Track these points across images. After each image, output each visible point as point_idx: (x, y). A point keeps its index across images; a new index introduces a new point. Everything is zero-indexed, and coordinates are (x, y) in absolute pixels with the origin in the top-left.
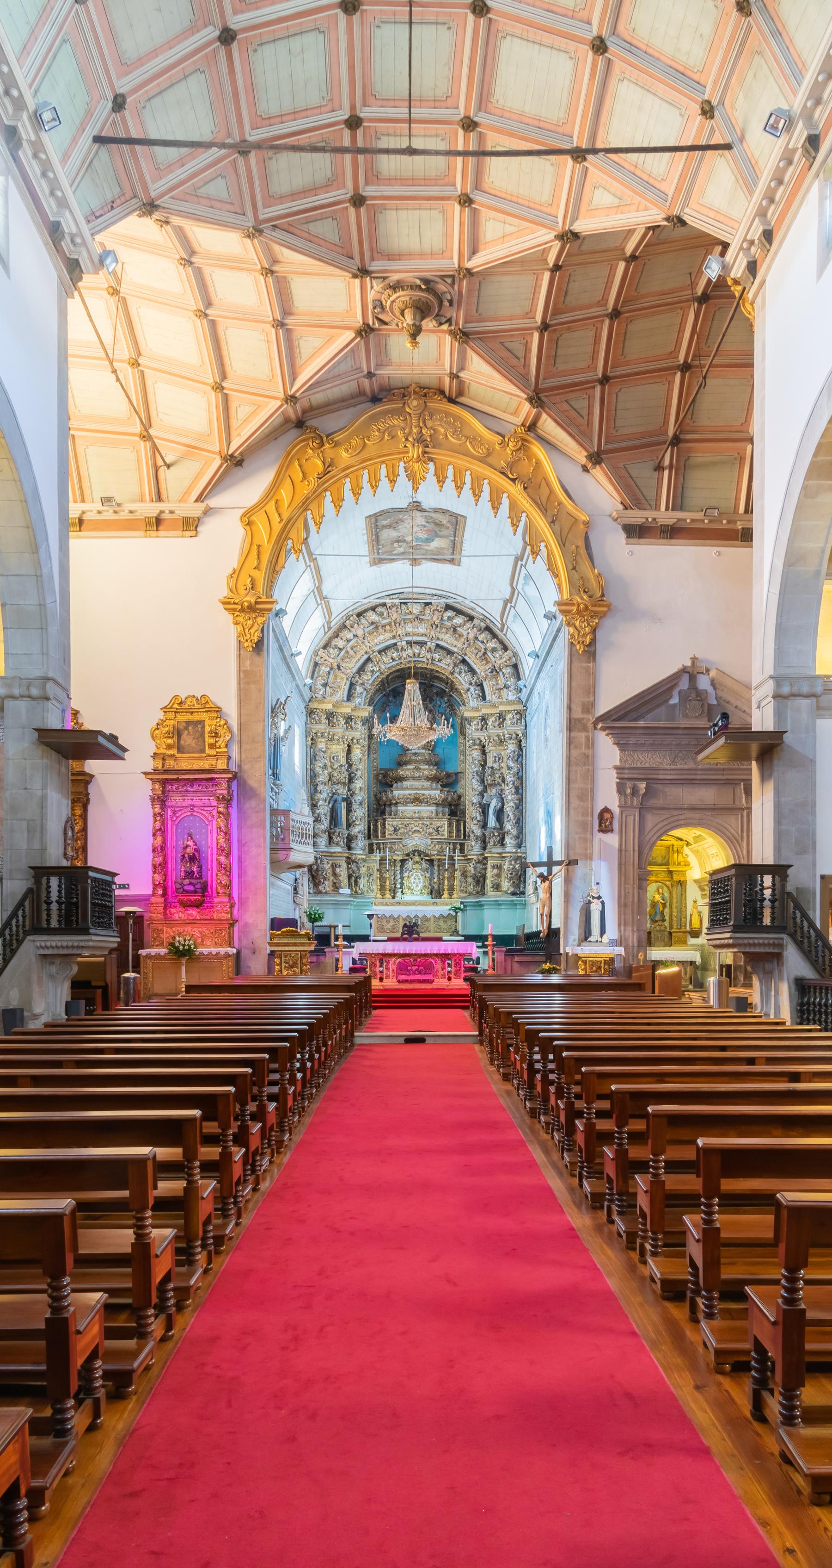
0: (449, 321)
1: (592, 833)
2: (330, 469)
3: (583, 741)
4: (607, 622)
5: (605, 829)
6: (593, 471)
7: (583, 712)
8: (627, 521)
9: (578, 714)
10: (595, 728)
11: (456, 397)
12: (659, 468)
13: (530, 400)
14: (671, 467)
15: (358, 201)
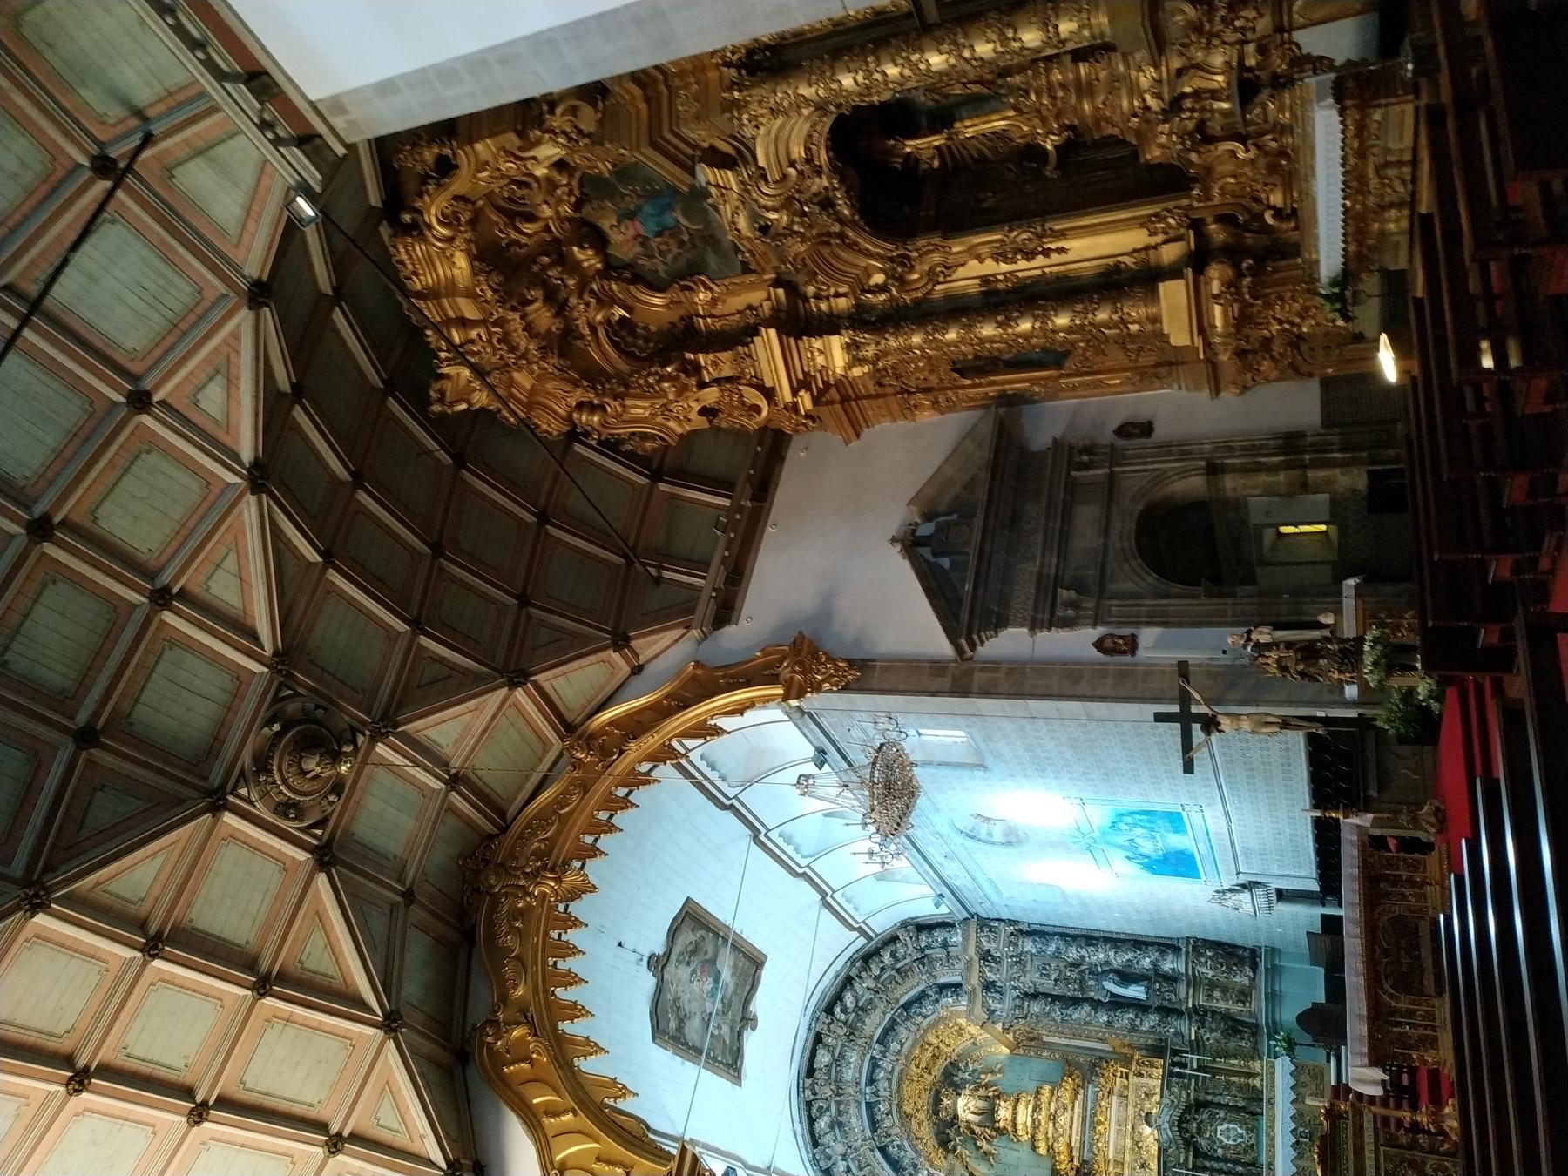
0: (354, 731)
1: (1135, 665)
2: (529, 1015)
3: (985, 675)
4: (828, 645)
5: (1132, 645)
6: (642, 659)
7: (944, 676)
8: (709, 618)
9: (946, 682)
10: (971, 659)
11: (505, 822)
12: (658, 581)
13: (513, 685)
14: (660, 568)
15: (87, 737)
